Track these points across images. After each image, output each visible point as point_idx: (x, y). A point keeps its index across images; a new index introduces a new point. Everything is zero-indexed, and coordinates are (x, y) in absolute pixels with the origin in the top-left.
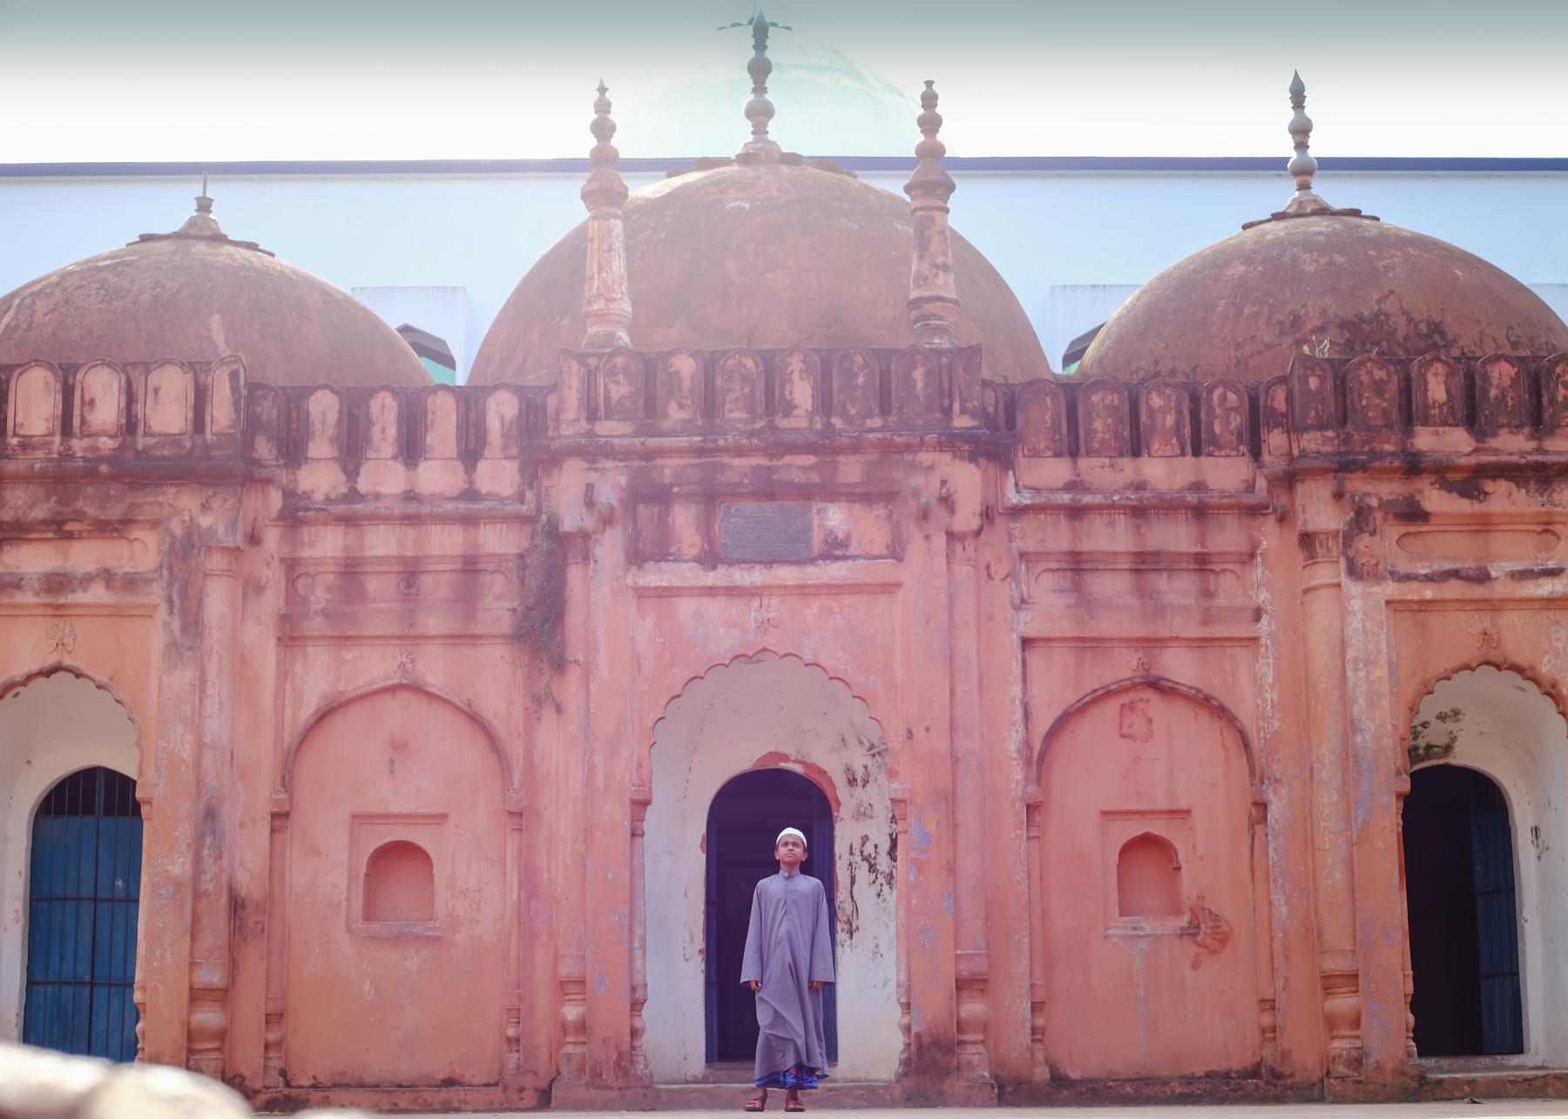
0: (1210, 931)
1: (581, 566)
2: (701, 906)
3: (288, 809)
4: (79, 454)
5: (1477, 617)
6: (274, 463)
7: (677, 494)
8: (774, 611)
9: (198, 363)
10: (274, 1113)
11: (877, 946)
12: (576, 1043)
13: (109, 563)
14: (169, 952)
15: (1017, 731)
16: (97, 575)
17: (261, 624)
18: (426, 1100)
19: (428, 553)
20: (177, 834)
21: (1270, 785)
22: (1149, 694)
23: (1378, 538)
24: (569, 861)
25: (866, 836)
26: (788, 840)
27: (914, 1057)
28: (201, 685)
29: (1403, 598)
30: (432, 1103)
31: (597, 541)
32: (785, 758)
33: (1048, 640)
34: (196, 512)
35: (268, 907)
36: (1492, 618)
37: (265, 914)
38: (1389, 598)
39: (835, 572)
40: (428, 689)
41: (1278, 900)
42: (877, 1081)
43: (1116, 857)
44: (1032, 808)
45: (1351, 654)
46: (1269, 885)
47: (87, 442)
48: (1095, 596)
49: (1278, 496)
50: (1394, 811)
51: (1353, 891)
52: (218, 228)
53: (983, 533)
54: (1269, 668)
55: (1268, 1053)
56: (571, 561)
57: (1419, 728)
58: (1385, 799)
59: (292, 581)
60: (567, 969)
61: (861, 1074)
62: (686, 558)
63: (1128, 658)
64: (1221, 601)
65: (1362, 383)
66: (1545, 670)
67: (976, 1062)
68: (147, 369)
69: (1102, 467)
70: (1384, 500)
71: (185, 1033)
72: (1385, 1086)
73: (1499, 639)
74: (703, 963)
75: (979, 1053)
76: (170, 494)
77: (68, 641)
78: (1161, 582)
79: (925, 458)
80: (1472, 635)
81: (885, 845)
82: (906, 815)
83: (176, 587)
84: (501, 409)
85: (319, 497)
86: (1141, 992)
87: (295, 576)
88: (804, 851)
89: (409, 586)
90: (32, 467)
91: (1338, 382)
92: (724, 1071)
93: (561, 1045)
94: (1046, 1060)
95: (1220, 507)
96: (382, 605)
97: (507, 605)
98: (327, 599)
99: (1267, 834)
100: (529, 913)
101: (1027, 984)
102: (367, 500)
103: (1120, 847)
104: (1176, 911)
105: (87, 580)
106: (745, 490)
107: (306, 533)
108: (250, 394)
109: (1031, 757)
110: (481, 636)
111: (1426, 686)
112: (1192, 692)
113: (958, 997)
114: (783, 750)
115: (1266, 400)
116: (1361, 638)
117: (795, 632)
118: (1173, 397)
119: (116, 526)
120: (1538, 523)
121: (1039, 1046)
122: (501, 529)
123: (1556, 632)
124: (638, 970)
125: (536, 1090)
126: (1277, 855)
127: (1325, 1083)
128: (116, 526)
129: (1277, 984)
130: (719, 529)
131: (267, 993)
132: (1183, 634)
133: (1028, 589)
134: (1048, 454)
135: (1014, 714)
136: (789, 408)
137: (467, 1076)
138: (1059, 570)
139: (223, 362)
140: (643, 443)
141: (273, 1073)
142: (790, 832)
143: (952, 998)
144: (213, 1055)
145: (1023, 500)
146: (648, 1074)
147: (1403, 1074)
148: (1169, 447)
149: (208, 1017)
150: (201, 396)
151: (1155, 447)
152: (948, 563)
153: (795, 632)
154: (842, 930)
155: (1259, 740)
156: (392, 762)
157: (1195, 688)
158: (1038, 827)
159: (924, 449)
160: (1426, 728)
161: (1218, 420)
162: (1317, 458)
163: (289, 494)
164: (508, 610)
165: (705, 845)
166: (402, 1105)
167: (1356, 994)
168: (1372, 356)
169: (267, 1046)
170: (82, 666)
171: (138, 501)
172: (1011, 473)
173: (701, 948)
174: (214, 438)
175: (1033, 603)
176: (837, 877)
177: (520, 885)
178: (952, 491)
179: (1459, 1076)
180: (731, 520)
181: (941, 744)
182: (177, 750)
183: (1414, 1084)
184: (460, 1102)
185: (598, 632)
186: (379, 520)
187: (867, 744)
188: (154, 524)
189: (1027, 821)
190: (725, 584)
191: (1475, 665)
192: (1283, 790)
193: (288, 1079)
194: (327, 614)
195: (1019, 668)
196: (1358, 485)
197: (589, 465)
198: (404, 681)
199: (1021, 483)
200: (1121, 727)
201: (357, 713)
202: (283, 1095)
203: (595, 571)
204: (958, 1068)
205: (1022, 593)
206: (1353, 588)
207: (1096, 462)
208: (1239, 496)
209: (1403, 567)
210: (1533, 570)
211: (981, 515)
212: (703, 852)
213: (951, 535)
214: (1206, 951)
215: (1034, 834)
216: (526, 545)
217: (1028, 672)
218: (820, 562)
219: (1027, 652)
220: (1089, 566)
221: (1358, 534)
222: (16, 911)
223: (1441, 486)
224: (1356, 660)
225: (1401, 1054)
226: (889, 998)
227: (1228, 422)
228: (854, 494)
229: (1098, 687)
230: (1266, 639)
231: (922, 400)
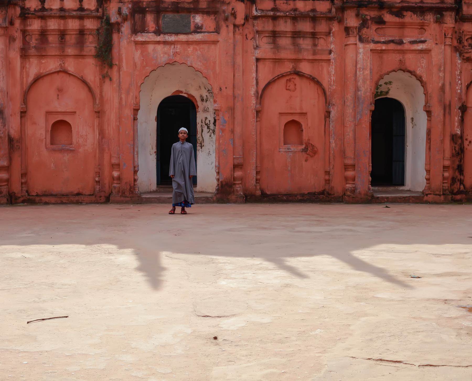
0: (311, 150)
1: (117, 34)
2: (155, 138)
5: (398, 55)
7: (148, 10)
8: (179, 49)
11: (209, 152)
15: (254, 88)
17: (15, 51)
19: (68, 28)
21: (332, 106)
22: (295, 76)
23: (369, 29)
25: (207, 117)
26: (182, 132)
29: (376, 49)
31: (122, 26)
32: (182, 92)
35: (20, 141)
36: (403, 56)
37: (20, 143)
38: (371, 49)
39: (198, 37)
40: (69, 72)
41: (332, 141)
43: (283, 127)
44: (258, 112)
45: (359, 66)
46: (330, 137)
48: (280, 45)
49: (339, 14)
54: (333, 69)
55: (327, 187)
56: (114, 32)
57: (379, 87)
58: (366, 112)
59: (24, 37)
60: (114, 161)
63: (289, 65)
64: (319, 48)
66: (418, 72)
67: (239, 190)
69: (283, 3)
70: (372, 17)
72: (361, 199)
73: (405, 63)
74: (156, 156)
75: (239, 187)
78: (301, 41)
80: (396, 60)
82: (219, 114)
85: (32, 9)
86: (289, 168)
87: (26, 35)
88: (187, 135)
89: (62, 39)
93: (112, 183)
94: (260, 188)
96: (54, 45)
97: (94, 45)
98: (35, 43)
99: (330, 121)
100: (102, 143)
101: (255, 166)
102: (48, 11)
103: (285, 123)
104: (301, 143)
106: (169, 10)
107: (29, 21)
110: (85, 56)
111: (381, 77)
112: (309, 76)
114: (181, 89)
116: (362, 61)
117: (185, 56)
120: (419, 26)
121: (258, 185)
122: (91, 21)
123: (422, 61)
125: (105, 197)
126: (333, 128)
127: (344, 197)
129: (331, 167)
130: (161, 22)
131: (21, 167)
132: (307, 58)
133: (259, 43)
135: (253, 82)
137: (84, 192)
138: (268, 36)
141: (24, 192)
142: (183, 129)
144: (5, 187)
145: (258, 14)
147: (367, 195)
152: (234, 34)
153: (185, 56)
154: (199, 146)
156: (58, 95)
162: (351, 3)
163: (23, 9)
164: (94, 47)
165: (156, 119)
166: (64, 201)
169: (22, 183)
172: (254, 5)
173: (155, 151)
175: (260, 47)
176: (197, 129)
177: (99, 134)
178: (235, 11)
179: (384, 196)
180: (165, 19)
181: (230, 92)
183: (370, 198)
184: (82, 200)
185: (123, 56)
186: (52, 17)
190: (163, 40)
191: (396, 70)
193: (29, 193)
194: (35, 47)
195: (255, 68)
196: (364, 12)
197: (119, 1)
198: (61, 70)
199: (257, 8)
200: (286, 87)
201: (47, 80)
203: (122, 35)
204: (233, 191)
206: (360, 45)
208: (326, 14)
209: (376, 39)
210: (417, 41)
211: (245, 19)
212: (156, 121)
213: (235, 26)
214: (309, 156)
215: (258, 120)
216: (99, 26)
217: (258, 69)
219: (258, 63)
220: (278, 35)
221: (363, 28)
224: (360, 68)
225: (367, 189)
226: (213, 168)
228: (204, 12)
229: (280, 74)
230: (333, 60)
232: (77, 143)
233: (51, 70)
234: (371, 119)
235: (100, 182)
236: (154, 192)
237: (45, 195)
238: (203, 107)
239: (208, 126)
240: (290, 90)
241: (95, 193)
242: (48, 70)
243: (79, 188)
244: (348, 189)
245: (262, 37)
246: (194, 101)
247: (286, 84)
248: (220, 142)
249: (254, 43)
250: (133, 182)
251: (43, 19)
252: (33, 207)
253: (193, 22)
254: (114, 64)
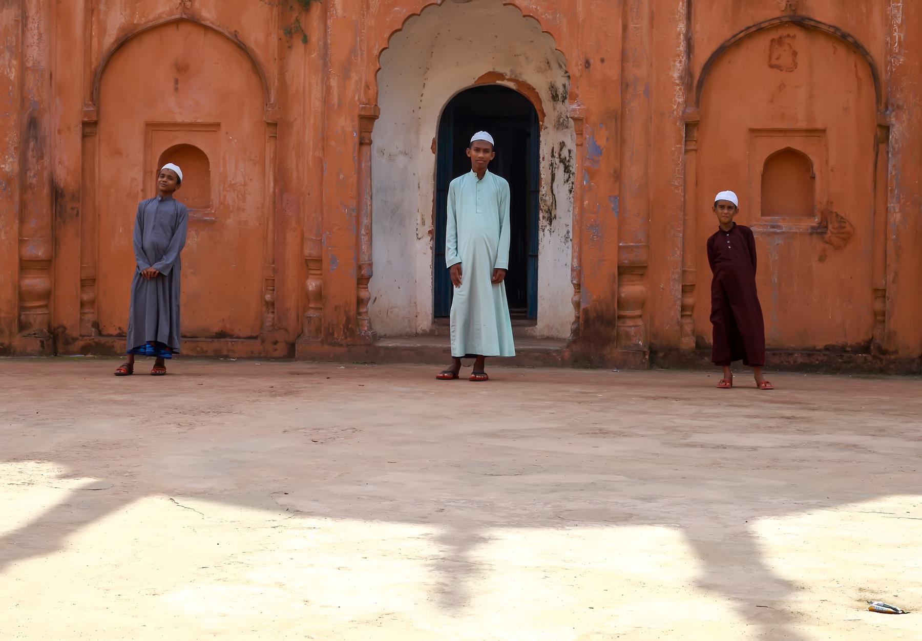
3: (95, 118)
10: (87, 356)
12: (316, 309)
14: (3, 231)
15: (680, 62)
20: (8, 139)
21: (893, 111)
24: (311, 164)
25: (563, 142)
28: (23, 20)
30: (207, 351)
37: (79, 201)
40: (203, 22)
41: (894, 208)
43: (760, 168)
44: (690, 126)
54: (898, 11)
60: (310, 250)
67: (632, 333)
71: (17, 295)
75: (635, 326)
82: (582, 131)
93: (306, 308)
94: (693, 331)
99: (888, 153)
101: (679, 270)
104: (810, 213)
109: (692, 83)
112: (832, 30)
113: (620, 280)
114: (499, 70)
121: (689, 320)
124: (364, 252)
125: (287, 343)
129: (888, 277)
131: (82, 263)
141: (87, 325)
143: (614, 282)
144: (39, 311)
149: (36, 282)
154: (544, 217)
155: (886, 71)
156: (177, 82)
158: (696, 141)
169: (83, 304)
177: (276, 181)
181: (613, 73)
182: (5, 73)
189: (686, 137)
192: (904, 116)
193: (100, 328)
200: (770, 58)
201: (150, 42)
202: (94, 342)
212: (434, 153)
217: (693, 11)
232: (221, 203)
233: (160, 17)
236: (425, 335)
238: (557, 114)
239: (565, 165)
240: (781, 67)
242: (151, 17)
243: (223, 320)
246: (533, 100)
247: (771, 50)
248: (583, 204)
250: (354, 306)
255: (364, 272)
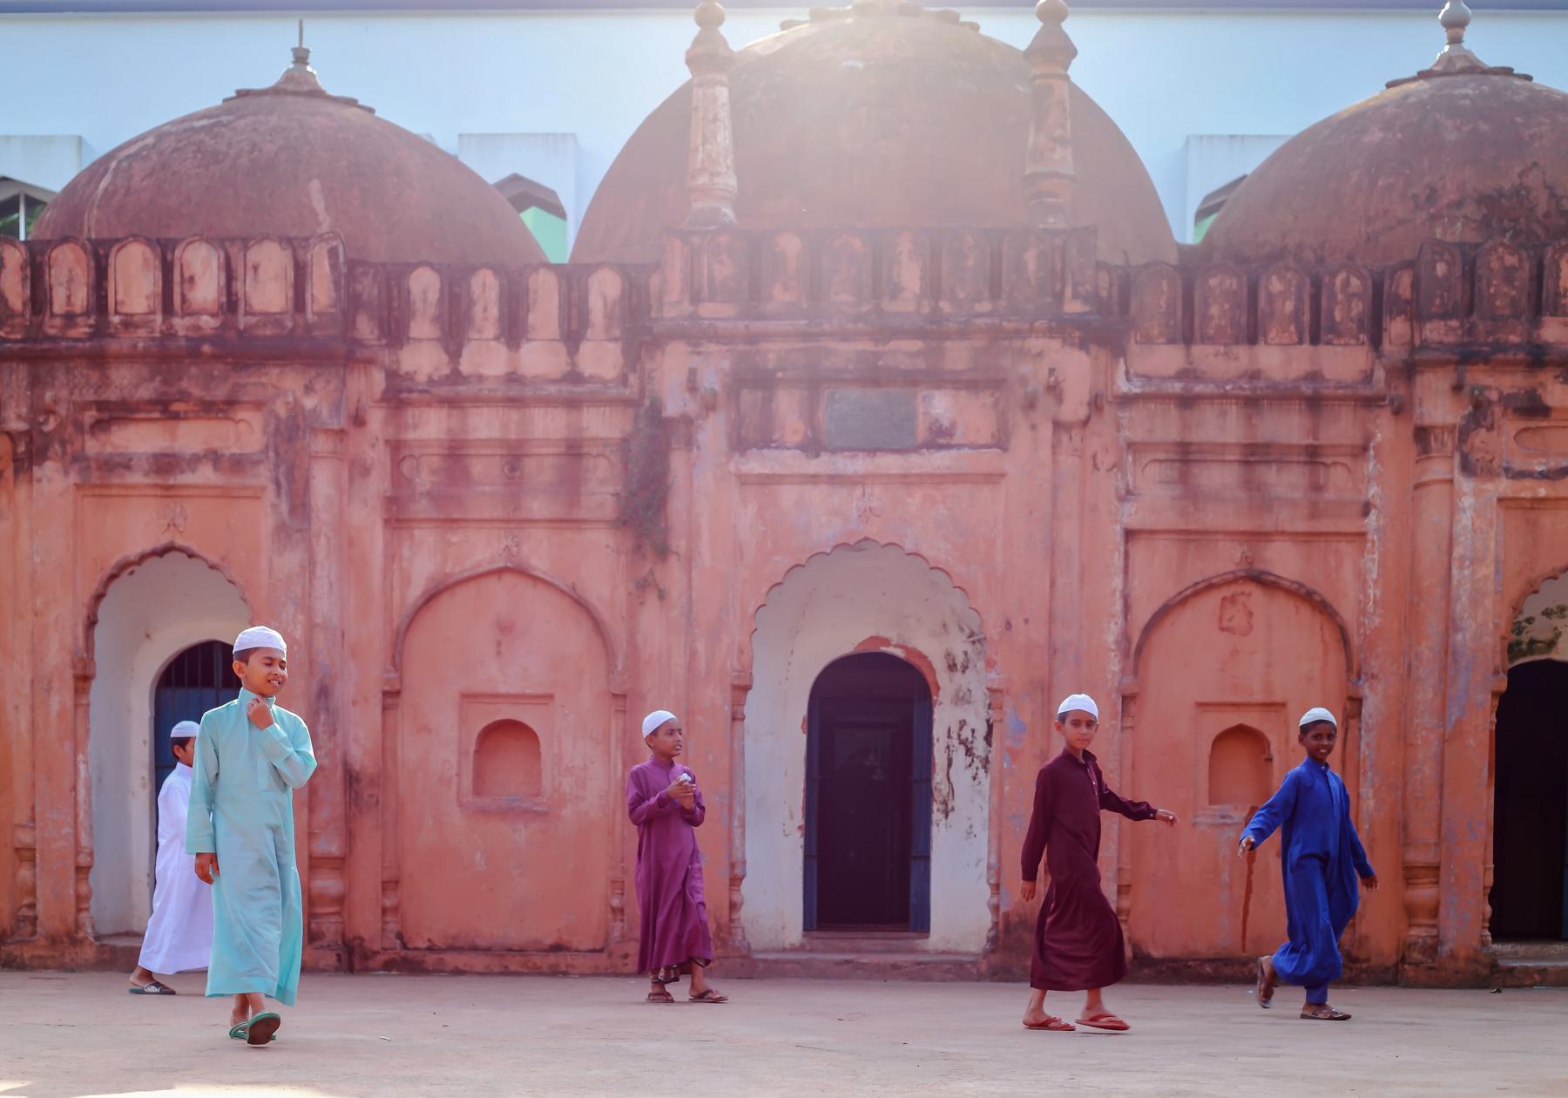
3: (398, 687)
4: (181, 333)
6: (376, 343)
9: (296, 238)
13: (216, 444)
15: (1116, 623)
16: (205, 456)
18: (535, 964)
21: (1367, 680)
27: (1001, 935)
28: (310, 565)
29: (1516, 495)
33: (1152, 532)
34: (299, 393)
38: (1503, 495)
42: (966, 954)
44: (1128, 699)
47: (188, 321)
49: (1396, 387)
50: (1488, 710)
51: (1441, 786)
52: (316, 83)
53: (1091, 424)
54: (1374, 564)
56: (674, 447)
61: (952, 946)
62: (788, 445)
64: (1330, 495)
65: (1491, 270)
68: (246, 243)
69: (1216, 355)
70: (1505, 393)
72: (1457, 972)
76: (272, 375)
77: (180, 521)
79: (1035, 344)
81: (982, 730)
83: (283, 469)
84: (604, 289)
86: (1225, 878)
87: (401, 457)
90: (135, 346)
91: (1467, 268)
92: (819, 941)
95: (1335, 398)
97: (610, 489)
99: (1360, 729)
101: (1114, 867)
105: (195, 461)
108: (349, 271)
110: (585, 521)
111: (1532, 586)
112: (1295, 586)
115: (1390, 287)
116: (1469, 536)
118: (1294, 282)
119: (221, 406)
128: (221, 406)
132: (1288, 528)
134: (1162, 340)
136: (896, 291)
137: (575, 944)
138: (1166, 461)
139: (321, 238)
140: (747, 327)
145: (1132, 388)
146: (746, 945)
148: (1286, 335)
149: (328, 884)
150: (301, 274)
151: (1272, 334)
157: (1297, 583)
158: (1133, 717)
159: (1034, 335)
160: (1530, 623)
161: (1340, 306)
164: (612, 495)
166: (513, 968)
167: (1435, 885)
168: (1505, 241)
169: (384, 911)
170: (194, 546)
171: (242, 381)
172: (1122, 361)
174: (316, 318)
175: (1139, 495)
178: (1061, 379)
182: (289, 630)
184: (567, 966)
187: (967, 631)
188: (258, 405)
193: (406, 937)
195: (1122, 559)
197: (690, 349)
198: (509, 565)
199: (1131, 371)
200: (1221, 619)
205: (1128, 485)
207: (1210, 349)
211: (1089, 404)
215: (1129, 724)
216: (629, 428)
217: (1130, 564)
218: (924, 451)
219: (1130, 545)
221: (1475, 429)
222: (143, 778)
223: (1564, 378)
225: (1476, 944)
227: (1349, 309)
231: (1033, 283)
234: (1495, 720)
235: (626, 912)
237: (452, 948)
241: (608, 945)
244: (1416, 943)
245: (1145, 462)
249: (1117, 480)
251: (456, 408)
252: (419, 979)
253: (925, 414)
254: (674, 548)
255: (738, 871)
